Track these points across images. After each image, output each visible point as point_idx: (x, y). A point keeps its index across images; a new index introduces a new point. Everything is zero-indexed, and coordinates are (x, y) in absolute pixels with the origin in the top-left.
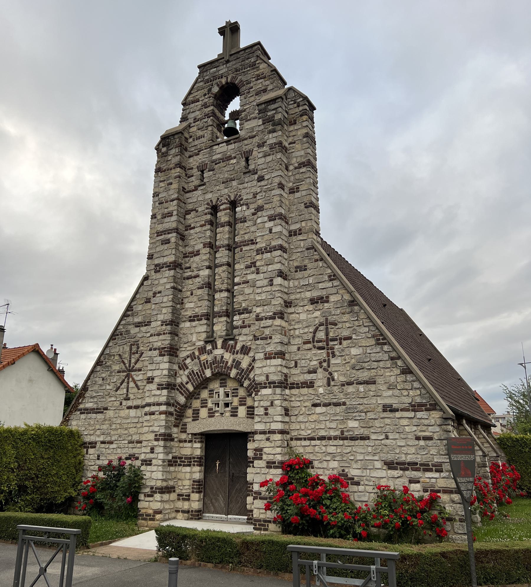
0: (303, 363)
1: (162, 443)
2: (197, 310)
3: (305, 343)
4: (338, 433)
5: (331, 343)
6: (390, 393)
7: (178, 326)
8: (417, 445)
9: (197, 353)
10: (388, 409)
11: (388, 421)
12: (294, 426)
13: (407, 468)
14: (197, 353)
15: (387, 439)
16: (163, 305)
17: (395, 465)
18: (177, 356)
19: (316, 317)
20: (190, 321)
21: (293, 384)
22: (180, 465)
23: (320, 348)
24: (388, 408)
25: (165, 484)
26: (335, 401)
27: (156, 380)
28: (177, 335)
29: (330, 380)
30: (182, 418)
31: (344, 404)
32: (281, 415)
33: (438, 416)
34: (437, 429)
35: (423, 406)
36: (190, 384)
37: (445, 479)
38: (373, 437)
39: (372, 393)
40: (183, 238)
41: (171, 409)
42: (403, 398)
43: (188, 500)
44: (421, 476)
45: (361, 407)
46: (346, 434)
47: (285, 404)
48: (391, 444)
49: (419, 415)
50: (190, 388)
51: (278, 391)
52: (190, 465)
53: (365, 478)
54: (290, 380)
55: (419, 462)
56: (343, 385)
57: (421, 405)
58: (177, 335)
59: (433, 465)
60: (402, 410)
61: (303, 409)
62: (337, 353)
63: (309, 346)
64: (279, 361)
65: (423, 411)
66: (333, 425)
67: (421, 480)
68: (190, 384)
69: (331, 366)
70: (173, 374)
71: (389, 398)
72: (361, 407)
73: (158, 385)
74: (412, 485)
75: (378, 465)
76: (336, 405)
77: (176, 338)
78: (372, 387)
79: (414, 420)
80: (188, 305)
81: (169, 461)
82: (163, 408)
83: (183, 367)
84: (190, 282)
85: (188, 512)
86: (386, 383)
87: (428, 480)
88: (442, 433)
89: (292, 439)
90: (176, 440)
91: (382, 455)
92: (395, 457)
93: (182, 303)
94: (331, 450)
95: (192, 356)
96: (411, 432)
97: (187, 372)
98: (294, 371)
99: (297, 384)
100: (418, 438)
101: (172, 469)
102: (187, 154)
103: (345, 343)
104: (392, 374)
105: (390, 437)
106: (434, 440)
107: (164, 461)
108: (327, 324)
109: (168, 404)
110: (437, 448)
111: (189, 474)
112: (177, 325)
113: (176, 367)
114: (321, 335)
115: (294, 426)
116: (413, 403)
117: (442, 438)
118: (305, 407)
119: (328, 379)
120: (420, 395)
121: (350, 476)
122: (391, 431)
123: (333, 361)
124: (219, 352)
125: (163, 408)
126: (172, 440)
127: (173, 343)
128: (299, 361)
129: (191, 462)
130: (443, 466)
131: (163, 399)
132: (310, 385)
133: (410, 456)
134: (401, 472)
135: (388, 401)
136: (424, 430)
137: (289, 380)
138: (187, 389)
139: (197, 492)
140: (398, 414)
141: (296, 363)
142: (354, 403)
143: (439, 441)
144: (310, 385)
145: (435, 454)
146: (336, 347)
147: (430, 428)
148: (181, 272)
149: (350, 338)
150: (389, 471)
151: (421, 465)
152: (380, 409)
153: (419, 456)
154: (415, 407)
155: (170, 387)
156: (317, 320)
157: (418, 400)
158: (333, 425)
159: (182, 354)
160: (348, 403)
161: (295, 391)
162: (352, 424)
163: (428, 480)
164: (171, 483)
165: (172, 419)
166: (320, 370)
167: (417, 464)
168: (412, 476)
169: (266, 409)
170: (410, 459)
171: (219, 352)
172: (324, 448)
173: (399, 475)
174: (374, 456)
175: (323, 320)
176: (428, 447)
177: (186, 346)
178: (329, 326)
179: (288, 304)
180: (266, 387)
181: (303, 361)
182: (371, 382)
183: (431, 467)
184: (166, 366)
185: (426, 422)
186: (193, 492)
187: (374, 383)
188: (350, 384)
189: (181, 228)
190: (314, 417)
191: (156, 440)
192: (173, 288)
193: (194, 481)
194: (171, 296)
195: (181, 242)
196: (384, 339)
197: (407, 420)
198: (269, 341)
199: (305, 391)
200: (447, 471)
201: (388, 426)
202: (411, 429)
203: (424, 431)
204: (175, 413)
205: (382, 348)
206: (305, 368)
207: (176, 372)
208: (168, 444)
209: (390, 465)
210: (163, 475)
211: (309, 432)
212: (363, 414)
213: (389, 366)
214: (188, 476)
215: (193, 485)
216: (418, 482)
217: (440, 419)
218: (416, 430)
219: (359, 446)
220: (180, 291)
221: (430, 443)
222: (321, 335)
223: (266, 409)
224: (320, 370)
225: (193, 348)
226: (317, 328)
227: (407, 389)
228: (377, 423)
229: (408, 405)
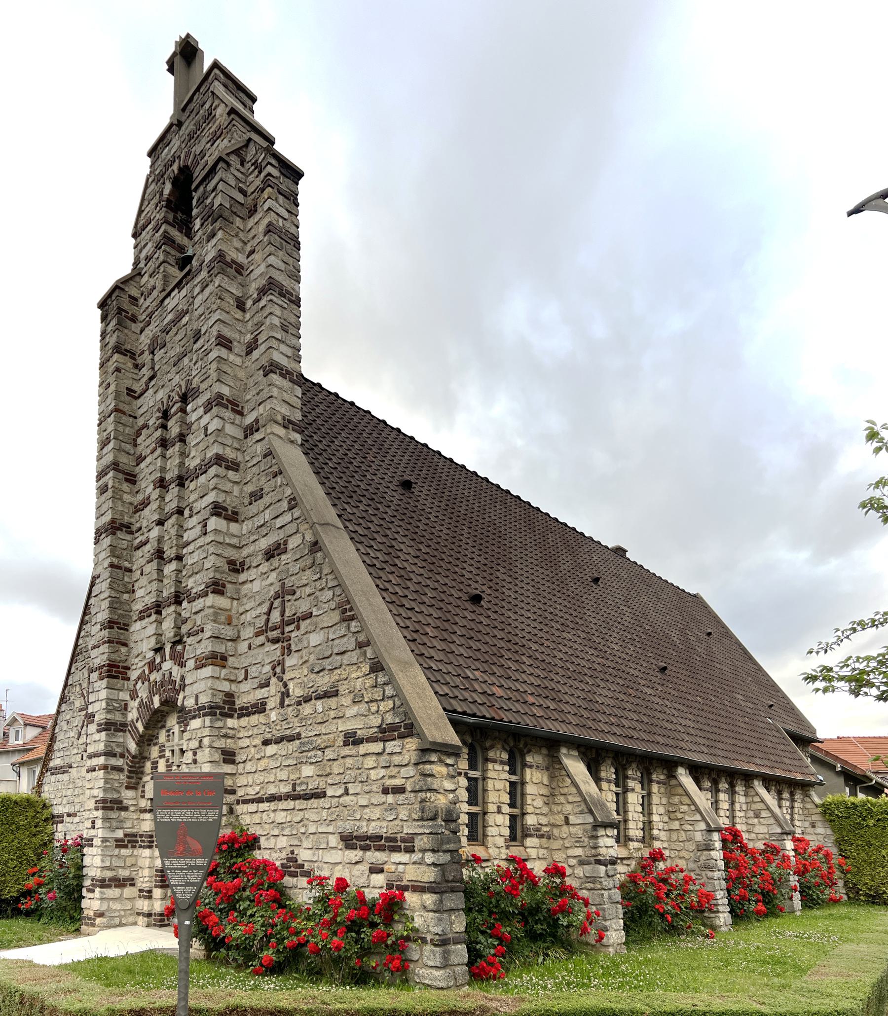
0: (253, 671)
1: (100, 814)
2: (147, 599)
3: (257, 635)
4: (285, 789)
5: (287, 629)
6: (355, 710)
7: (127, 630)
8: (384, 803)
9: (147, 672)
10: (351, 740)
11: (349, 762)
12: (241, 781)
13: (368, 845)
14: (147, 672)
15: (348, 794)
16: (102, 596)
17: (354, 841)
18: (128, 679)
19: (272, 584)
20: (141, 619)
21: (242, 708)
22: (140, 847)
23: (275, 641)
24: (352, 739)
25: (109, 874)
26: (288, 732)
27: (96, 718)
28: (126, 645)
29: (285, 694)
30: (140, 775)
31: (298, 736)
32: (210, 762)
33: (414, 748)
34: (410, 771)
35: (395, 731)
36: (140, 721)
37: (417, 866)
38: (330, 792)
39: (332, 714)
41: (120, 762)
42: (372, 717)
43: (150, 897)
44: (386, 859)
45: (319, 740)
46: (298, 789)
47: (221, 743)
48: (352, 804)
49: (391, 746)
50: (140, 727)
51: (207, 719)
52: (150, 847)
53: (316, 864)
54: (239, 703)
55: (384, 835)
56: (299, 703)
57: (393, 728)
59: (403, 840)
60: (371, 740)
61: (253, 750)
62: (293, 648)
63: (262, 639)
64: (208, 671)
65: (394, 739)
66: (283, 775)
67: (386, 867)
68: (140, 721)
69: (287, 670)
70: (118, 707)
71: (353, 720)
72: (319, 740)
73: (99, 725)
74: (374, 876)
75: (334, 840)
76: (291, 739)
77: (124, 650)
78: (332, 702)
79: (385, 757)
81: (117, 840)
82: (101, 760)
83: (134, 695)
84: (139, 553)
85: (149, 915)
86: (350, 692)
87: (393, 868)
88: (418, 777)
89: (238, 802)
90: (132, 809)
91: (340, 823)
92: (355, 825)
93: (134, 591)
94: (281, 817)
95: (143, 678)
96: (377, 780)
97: (138, 700)
98: (245, 687)
99: (247, 708)
100: (385, 791)
101: (124, 852)
103: (304, 625)
104: (359, 674)
105: (351, 792)
106: (407, 793)
107: (104, 840)
108: (284, 593)
109: (109, 754)
110: (409, 807)
111: (148, 860)
112: (125, 627)
113: (124, 696)
114: (276, 617)
115: (241, 781)
116: (384, 726)
117: (417, 788)
118: (255, 746)
119: (283, 693)
120: (394, 708)
121: (299, 862)
122: (353, 780)
123: (290, 662)
124: (167, 665)
125: (101, 760)
126: (126, 809)
128: (249, 668)
129: (153, 842)
130: (416, 841)
131: (101, 747)
132: (260, 708)
133: (373, 824)
134: (361, 853)
135: (349, 726)
136: (393, 774)
137: (237, 702)
138: (136, 728)
139: (162, 887)
140: (363, 748)
141: (246, 672)
142: (310, 734)
143: (412, 795)
144: (260, 708)
145: (406, 819)
146: (293, 635)
147: (403, 770)
149: (309, 616)
150: (347, 852)
151: (389, 839)
152: (340, 741)
153: (384, 824)
154: (386, 733)
155: (108, 727)
156: (272, 588)
157: (390, 719)
158: (283, 775)
159: (134, 675)
160: (303, 735)
161: (244, 721)
162: (307, 771)
163: (393, 868)
164: (124, 873)
165: (123, 777)
166: (274, 680)
167: (380, 838)
168: (374, 860)
169: (195, 754)
170: (372, 829)
171: (167, 665)
172: (272, 815)
173: (357, 859)
174: (328, 825)
175: (277, 587)
176: (398, 807)
177: (136, 661)
178: (287, 597)
179: (237, 567)
180: (194, 717)
181: (254, 668)
182: (331, 693)
183: (399, 843)
184: (103, 694)
185: (396, 759)
186: (156, 886)
187: (336, 694)
188: (307, 700)
190: (262, 764)
191: (97, 809)
193: (157, 871)
194: (109, 580)
196: (351, 609)
197: (374, 758)
198: (200, 636)
199: (254, 719)
200: (420, 851)
201: (349, 772)
202: (378, 774)
203: (394, 777)
204: (126, 767)
205: (349, 627)
206: (256, 680)
207: (126, 705)
208: (113, 815)
209: (349, 841)
210: (103, 861)
211: (257, 789)
212: (320, 753)
213: (354, 660)
214: (147, 862)
215: (157, 876)
216: (381, 871)
217: (417, 752)
218: (384, 777)
219: (314, 810)
221: (401, 798)
222: (276, 617)
223: (195, 754)
224: (274, 680)
225: (143, 663)
226: (272, 603)
227: (377, 701)
228: (336, 768)
229: (376, 730)
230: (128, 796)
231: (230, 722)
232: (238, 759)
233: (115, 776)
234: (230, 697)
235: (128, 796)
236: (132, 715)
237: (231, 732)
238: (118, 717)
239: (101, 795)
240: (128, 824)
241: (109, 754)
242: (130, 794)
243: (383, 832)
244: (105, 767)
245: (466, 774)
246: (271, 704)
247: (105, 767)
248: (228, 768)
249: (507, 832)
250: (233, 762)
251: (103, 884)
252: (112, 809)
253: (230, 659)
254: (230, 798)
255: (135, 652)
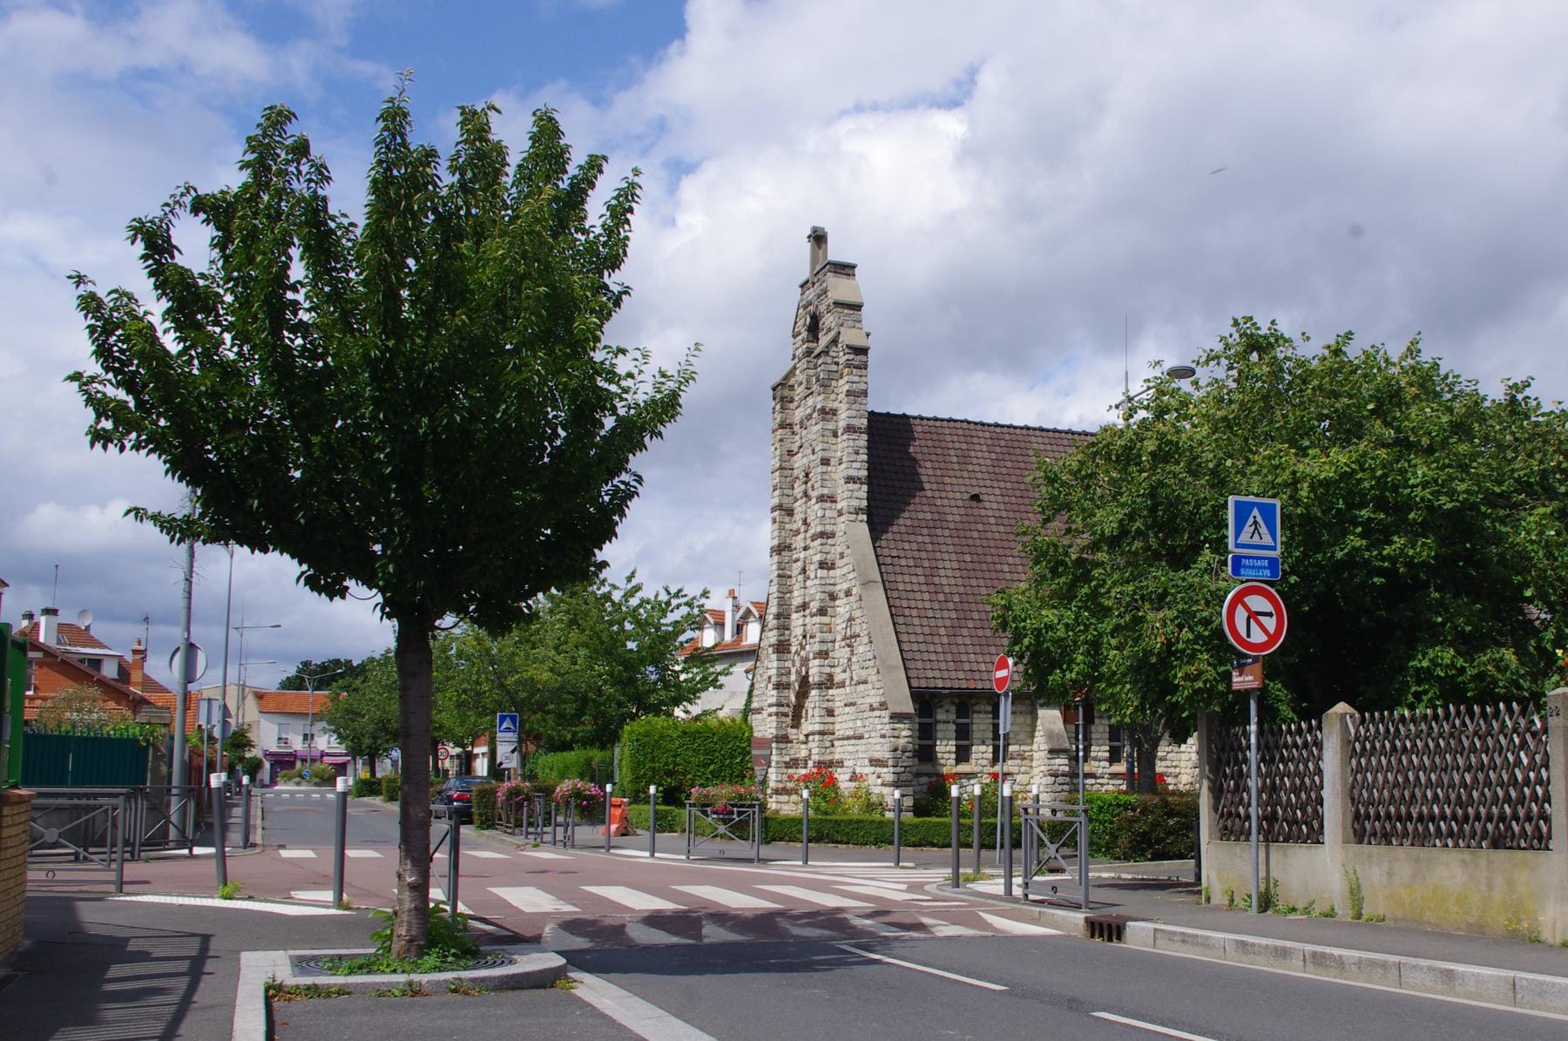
4: (851, 733)
25: (781, 785)
28: (789, 629)
40: (790, 512)
41: (785, 710)
47: (826, 705)
58: (789, 629)
77: (787, 632)
80: (796, 593)
81: (785, 763)
82: (774, 709)
102: (792, 406)
109: (779, 705)
112: (788, 617)
125: (774, 709)
126: (791, 742)
127: (782, 638)
131: (773, 700)
148: (790, 554)
158: (851, 724)
159: (793, 649)
165: (789, 720)
189: (786, 500)
192: (779, 576)
195: (787, 519)
220: (790, 577)
230: (792, 732)
231: (831, 692)
232: (836, 713)
233: (783, 719)
234: (831, 676)
235: (792, 732)
236: (793, 677)
237: (831, 698)
238: (784, 679)
239: (775, 732)
240: (793, 752)
241: (779, 705)
242: (794, 731)
243: (880, 757)
244: (777, 714)
245: (954, 722)
246: (847, 683)
247: (777, 714)
248: (830, 719)
249: (991, 756)
250: (833, 716)
251: (777, 792)
252: (782, 742)
253: (831, 654)
254: (831, 737)
255: (793, 634)
